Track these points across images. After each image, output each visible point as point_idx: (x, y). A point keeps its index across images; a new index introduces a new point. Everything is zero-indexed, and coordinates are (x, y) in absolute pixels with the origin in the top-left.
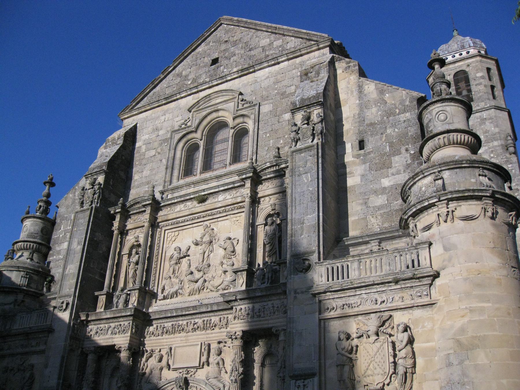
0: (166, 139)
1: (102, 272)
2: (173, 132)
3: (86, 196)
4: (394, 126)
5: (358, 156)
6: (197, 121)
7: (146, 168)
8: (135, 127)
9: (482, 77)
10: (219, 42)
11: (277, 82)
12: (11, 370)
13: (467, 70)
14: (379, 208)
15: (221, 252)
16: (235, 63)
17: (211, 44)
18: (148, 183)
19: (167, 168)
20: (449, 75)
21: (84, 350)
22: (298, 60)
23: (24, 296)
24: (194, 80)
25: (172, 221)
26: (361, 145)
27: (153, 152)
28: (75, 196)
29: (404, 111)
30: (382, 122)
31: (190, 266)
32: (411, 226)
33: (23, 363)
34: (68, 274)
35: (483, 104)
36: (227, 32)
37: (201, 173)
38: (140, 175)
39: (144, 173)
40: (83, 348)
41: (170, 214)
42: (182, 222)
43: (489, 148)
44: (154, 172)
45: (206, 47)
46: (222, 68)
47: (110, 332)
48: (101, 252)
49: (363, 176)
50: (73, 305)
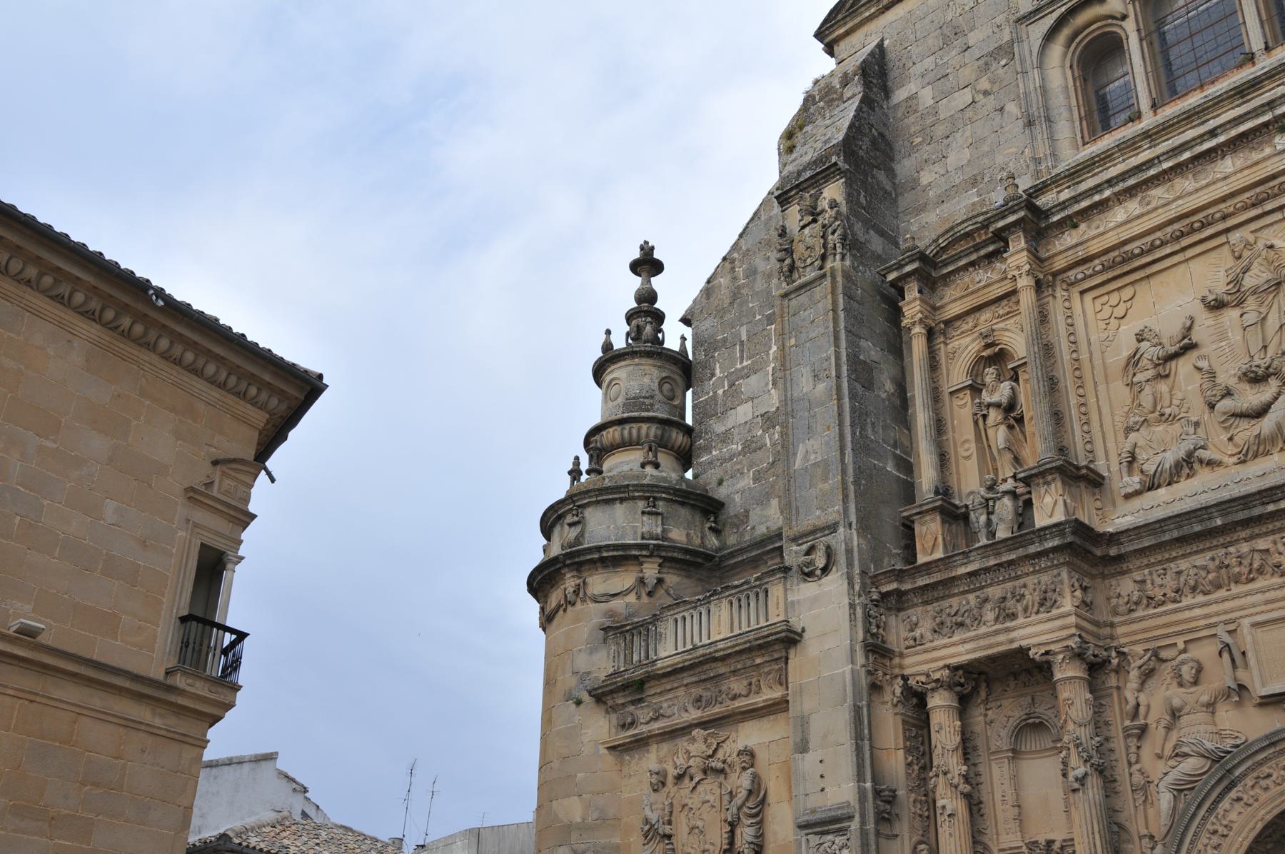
0: (1000, 48)
1: (898, 452)
3: (799, 249)
7: (954, 145)
8: (880, 46)
12: (679, 778)
18: (974, 182)
19: (1030, 124)
21: (912, 682)
23: (660, 565)
25: (1103, 258)
28: (735, 279)
31: (1212, 375)
33: (715, 751)
37: (1155, 107)
38: (938, 168)
39: (952, 160)
40: (905, 678)
41: (1094, 238)
42: (1143, 253)
44: (986, 148)
47: (989, 616)
48: (884, 396)
50: (849, 552)
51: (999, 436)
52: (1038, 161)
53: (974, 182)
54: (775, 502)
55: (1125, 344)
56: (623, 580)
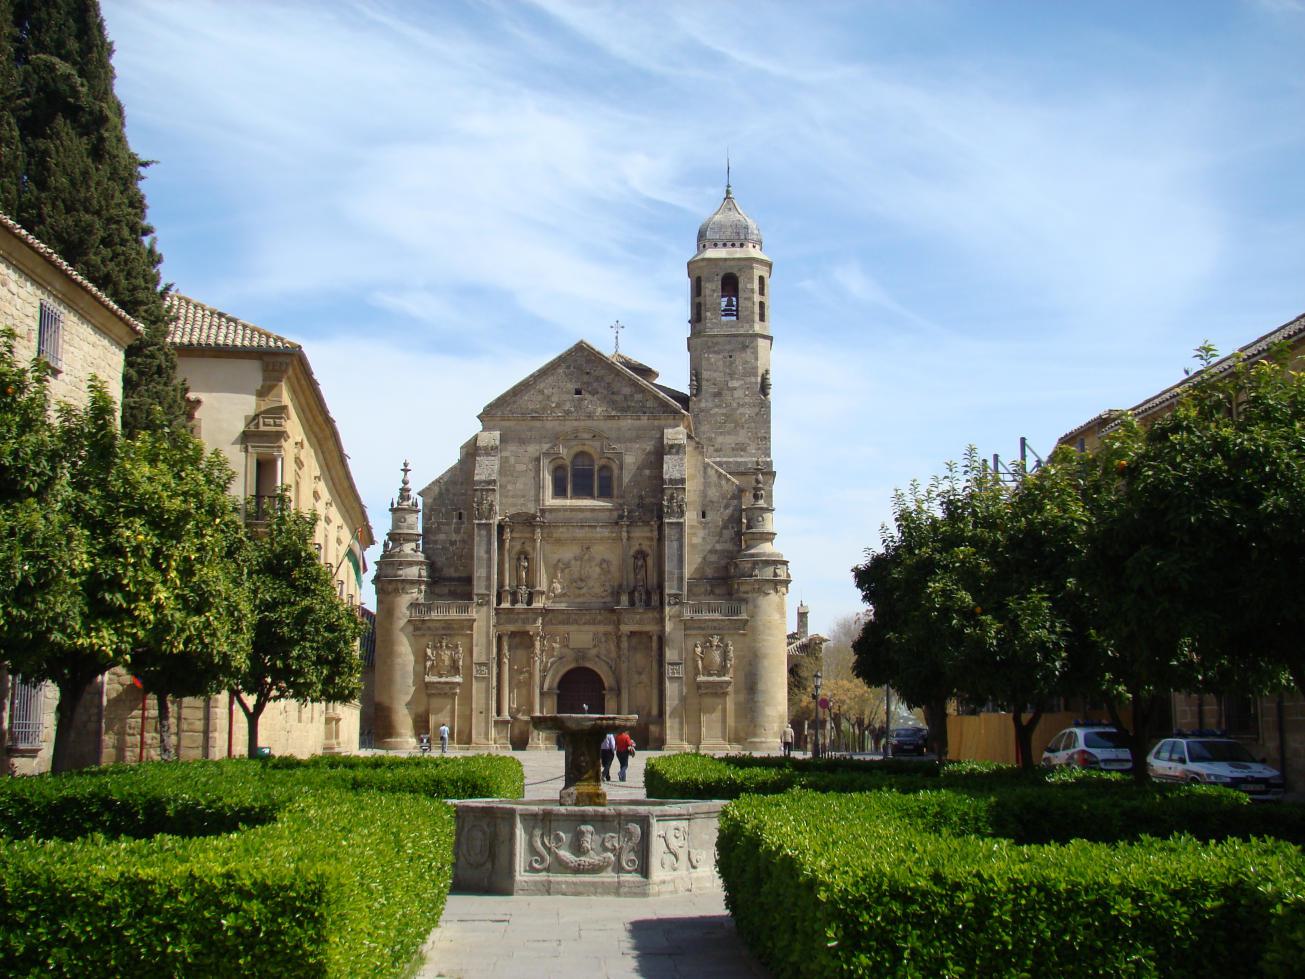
5: (701, 523)
9: (752, 291)
15: (598, 570)
17: (572, 369)
22: (656, 423)
24: (558, 405)
26: (704, 516)
27: (524, 467)
30: (718, 502)
32: (736, 586)
35: (748, 325)
36: (588, 361)
37: (571, 498)
49: (704, 538)
53: (523, 496)
54: (452, 570)
55: (555, 562)
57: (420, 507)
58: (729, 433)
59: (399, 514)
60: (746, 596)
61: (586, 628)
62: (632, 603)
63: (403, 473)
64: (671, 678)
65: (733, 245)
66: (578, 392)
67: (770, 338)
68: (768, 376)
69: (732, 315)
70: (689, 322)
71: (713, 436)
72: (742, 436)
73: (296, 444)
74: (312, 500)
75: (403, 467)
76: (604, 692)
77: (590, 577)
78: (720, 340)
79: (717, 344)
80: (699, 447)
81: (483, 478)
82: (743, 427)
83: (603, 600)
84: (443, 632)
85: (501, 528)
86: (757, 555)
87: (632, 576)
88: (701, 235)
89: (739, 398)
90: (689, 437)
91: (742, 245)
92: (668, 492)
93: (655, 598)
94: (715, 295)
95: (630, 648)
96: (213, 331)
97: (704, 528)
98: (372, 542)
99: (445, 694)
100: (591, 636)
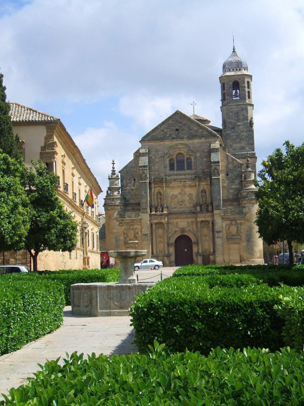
2: (165, 154)
4: (236, 171)
5: (226, 178)
6: (174, 152)
9: (245, 87)
10: (177, 121)
11: (201, 146)
13: (239, 81)
14: (232, 193)
15: (188, 198)
16: (185, 133)
19: (165, 167)
20: (231, 82)
22: (208, 140)
24: (170, 136)
27: (158, 160)
29: (239, 168)
30: (233, 169)
32: (241, 202)
34: (143, 202)
35: (243, 101)
36: (180, 118)
37: (177, 170)
43: (244, 123)
45: (173, 122)
46: (180, 134)
47: (159, 219)
49: (228, 184)
51: (159, 201)
52: (165, 172)
53: (158, 171)
54: (133, 200)
56: (119, 207)
57: (119, 177)
58: (238, 143)
59: (111, 180)
60: (245, 205)
61: (184, 220)
62: (201, 210)
63: (112, 164)
64: (218, 238)
65: (237, 70)
66: (177, 130)
67: (253, 105)
68: (252, 120)
69: (238, 97)
70: (221, 100)
71: (232, 144)
72: (243, 144)
73: (62, 156)
74: (71, 177)
75: (112, 162)
76: (192, 244)
77: (185, 201)
78: (233, 107)
79: (232, 108)
80: (224, 149)
81: (142, 165)
82: (243, 140)
83: (190, 209)
84: (130, 224)
85: (150, 183)
86: (250, 189)
87: (201, 200)
88: (224, 67)
89: (241, 129)
90: (221, 145)
91: (240, 70)
92: (213, 167)
93: (210, 208)
94: (230, 89)
95: (201, 227)
96: (28, 116)
97: (228, 180)
98: (102, 191)
99: (132, 247)
100: (186, 223)
